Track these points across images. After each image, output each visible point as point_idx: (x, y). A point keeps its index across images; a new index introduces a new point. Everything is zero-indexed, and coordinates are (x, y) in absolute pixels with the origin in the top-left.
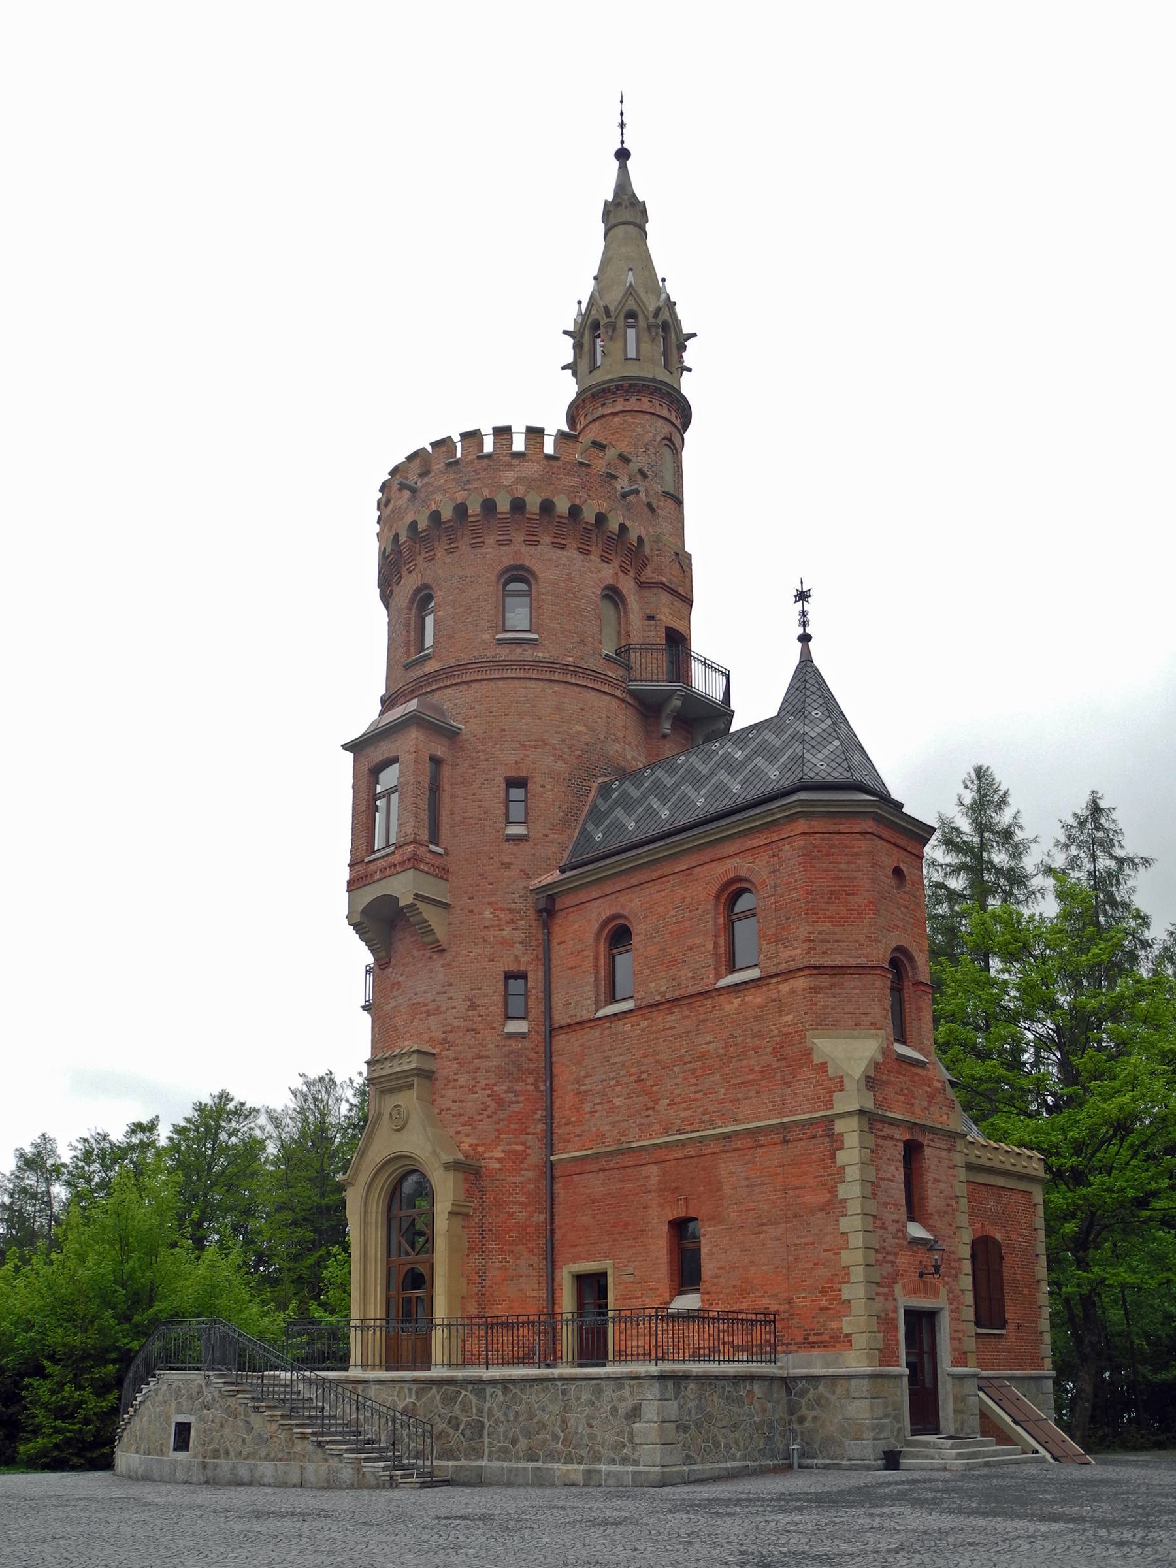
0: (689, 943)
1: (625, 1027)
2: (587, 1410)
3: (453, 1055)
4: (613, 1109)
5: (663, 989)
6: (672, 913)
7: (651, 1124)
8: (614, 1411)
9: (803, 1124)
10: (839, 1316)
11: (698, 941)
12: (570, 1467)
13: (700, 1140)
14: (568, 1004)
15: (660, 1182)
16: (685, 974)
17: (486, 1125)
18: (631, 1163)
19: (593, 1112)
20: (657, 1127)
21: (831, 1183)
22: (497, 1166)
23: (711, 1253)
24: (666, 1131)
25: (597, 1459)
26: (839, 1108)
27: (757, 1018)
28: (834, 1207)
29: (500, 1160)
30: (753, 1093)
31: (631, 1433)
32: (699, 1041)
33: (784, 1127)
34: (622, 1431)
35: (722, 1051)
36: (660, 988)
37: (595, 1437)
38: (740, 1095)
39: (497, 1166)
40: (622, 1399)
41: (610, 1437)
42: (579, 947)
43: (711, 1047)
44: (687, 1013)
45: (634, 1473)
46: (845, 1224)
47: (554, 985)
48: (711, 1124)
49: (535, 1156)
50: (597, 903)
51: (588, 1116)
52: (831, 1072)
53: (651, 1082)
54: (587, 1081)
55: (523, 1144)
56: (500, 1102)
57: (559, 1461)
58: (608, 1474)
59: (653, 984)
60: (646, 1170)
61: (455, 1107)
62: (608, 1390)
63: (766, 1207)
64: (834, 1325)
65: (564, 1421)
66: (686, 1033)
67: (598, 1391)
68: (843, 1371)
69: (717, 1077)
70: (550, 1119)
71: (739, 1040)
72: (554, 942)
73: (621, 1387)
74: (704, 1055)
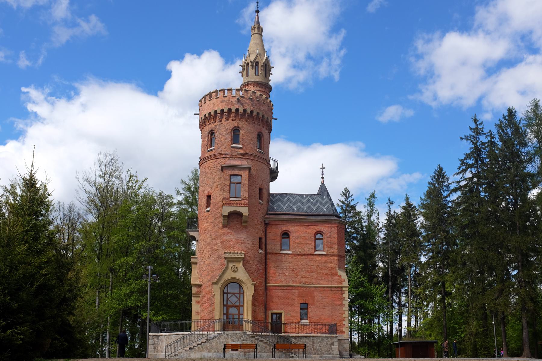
0: (308, 242)
1: (289, 257)
2: (319, 343)
3: (248, 255)
4: (285, 275)
5: (300, 251)
6: (303, 234)
7: (296, 281)
8: (327, 344)
9: (336, 287)
10: (343, 327)
11: (310, 242)
12: (316, 355)
13: (310, 287)
14: (272, 248)
15: (298, 294)
16: (306, 249)
17: (256, 274)
18: (290, 289)
19: (279, 275)
20: (298, 282)
21: (341, 300)
22: (258, 285)
23: (311, 312)
24: (300, 283)
25: (323, 353)
26: (344, 285)
27: (325, 263)
28: (342, 305)
29: (258, 283)
30: (323, 279)
31: (331, 348)
32: (310, 265)
33: (331, 287)
34: (329, 348)
35: (316, 268)
36: (299, 250)
37: (322, 349)
38: (320, 279)
39: (258, 285)
40: (329, 341)
41: (326, 349)
42: (276, 235)
43: (313, 267)
44: (307, 258)
45: (333, 356)
46: (344, 309)
47: (267, 242)
48: (313, 283)
49: (264, 284)
50: (281, 226)
51: (277, 276)
52: (342, 278)
53: (296, 271)
54: (278, 267)
55: (262, 280)
56: (258, 269)
57: (312, 354)
58: (326, 356)
59: (297, 249)
60: (294, 291)
61: (249, 269)
62: (325, 339)
63: (326, 303)
64: (341, 329)
65: (313, 346)
66: (306, 262)
67: (322, 340)
68: (343, 338)
69: (314, 273)
70: (266, 275)
71: (320, 266)
72: (268, 232)
73: (328, 338)
74: (311, 268)
